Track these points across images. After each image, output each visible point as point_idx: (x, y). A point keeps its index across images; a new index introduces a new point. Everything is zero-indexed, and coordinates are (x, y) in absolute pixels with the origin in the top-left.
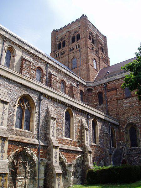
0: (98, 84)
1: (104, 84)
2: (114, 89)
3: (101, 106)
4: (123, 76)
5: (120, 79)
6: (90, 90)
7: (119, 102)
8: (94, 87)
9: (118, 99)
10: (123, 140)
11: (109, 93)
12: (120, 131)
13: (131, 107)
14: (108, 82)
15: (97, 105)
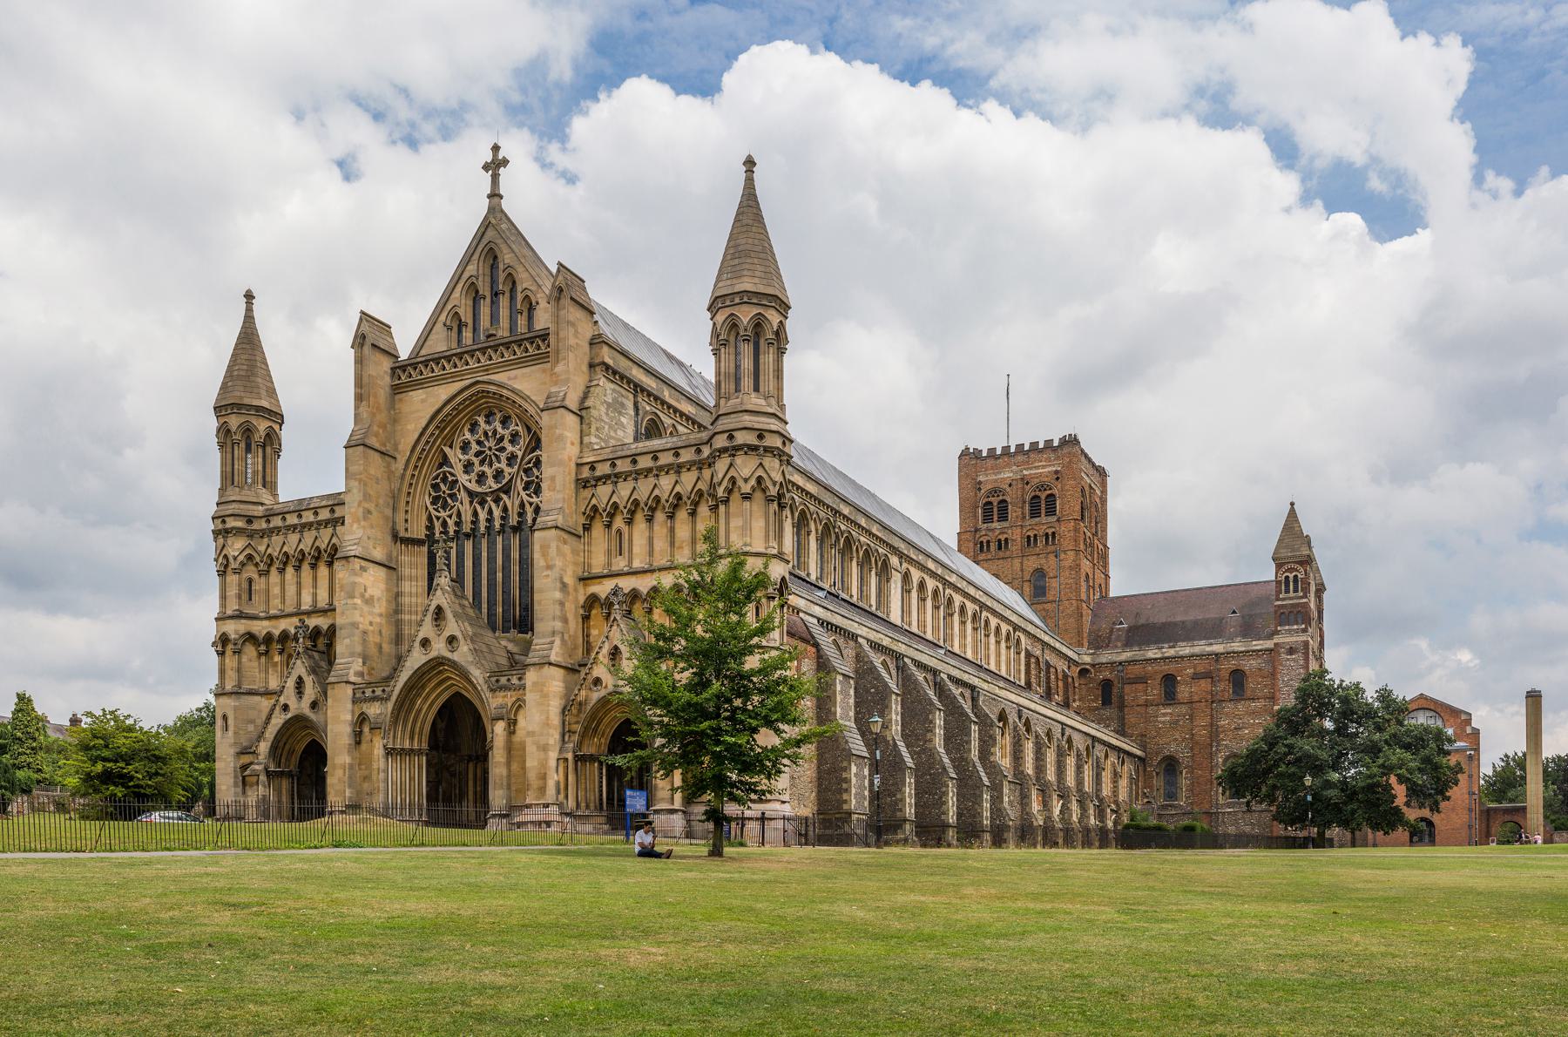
0: (1104, 661)
1: (1120, 663)
2: (1142, 680)
3: (1107, 712)
4: (1166, 655)
5: (1156, 659)
6: (1084, 672)
7: (1151, 710)
8: (1093, 666)
9: (1146, 704)
10: (1151, 787)
11: (1127, 688)
12: (1145, 770)
13: (1174, 724)
14: (1129, 662)
15: (1097, 709)
